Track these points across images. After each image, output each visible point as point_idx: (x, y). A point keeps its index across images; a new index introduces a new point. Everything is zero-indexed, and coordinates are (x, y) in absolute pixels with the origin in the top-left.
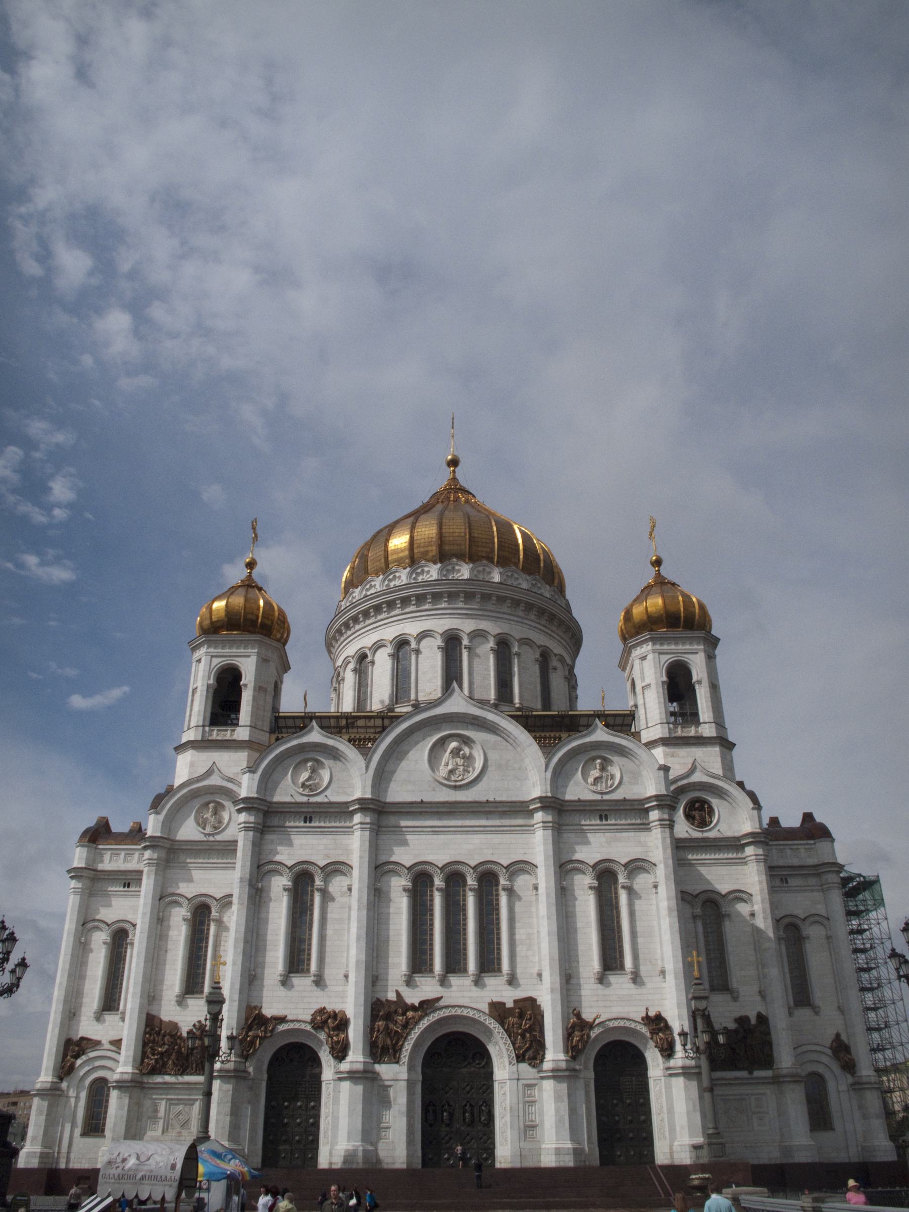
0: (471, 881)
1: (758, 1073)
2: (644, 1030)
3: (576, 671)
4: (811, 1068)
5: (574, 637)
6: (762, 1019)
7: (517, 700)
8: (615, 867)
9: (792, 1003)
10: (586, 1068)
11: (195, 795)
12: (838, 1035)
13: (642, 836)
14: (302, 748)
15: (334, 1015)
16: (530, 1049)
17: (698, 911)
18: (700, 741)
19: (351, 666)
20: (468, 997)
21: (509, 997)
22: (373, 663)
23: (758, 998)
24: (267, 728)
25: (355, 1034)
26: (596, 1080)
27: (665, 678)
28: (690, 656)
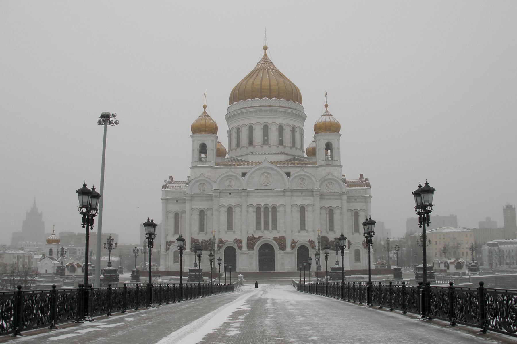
0: (270, 209)
2: (308, 243)
5: (303, 118)
7: (284, 144)
11: (197, 181)
13: (312, 198)
14: (228, 176)
15: (239, 240)
16: (283, 247)
17: (328, 212)
18: (332, 165)
19: (235, 130)
20: (269, 236)
21: (278, 236)
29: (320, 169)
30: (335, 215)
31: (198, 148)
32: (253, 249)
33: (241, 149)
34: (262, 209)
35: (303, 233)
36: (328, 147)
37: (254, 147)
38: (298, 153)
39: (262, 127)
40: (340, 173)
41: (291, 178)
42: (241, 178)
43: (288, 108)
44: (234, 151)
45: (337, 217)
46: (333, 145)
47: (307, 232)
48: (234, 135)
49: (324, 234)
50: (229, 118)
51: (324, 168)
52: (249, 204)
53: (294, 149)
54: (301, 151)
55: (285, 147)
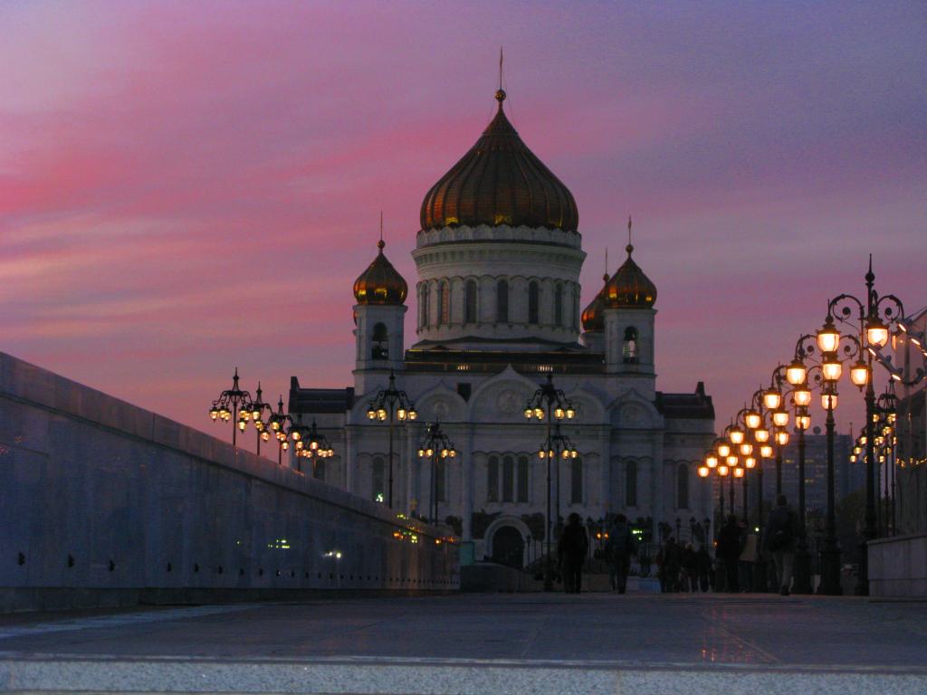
3: (581, 282)
5: (578, 259)
18: (638, 374)
19: (435, 287)
20: (513, 512)
21: (531, 511)
25: (466, 526)
32: (482, 538)
34: (501, 462)
36: (630, 333)
42: (460, 399)
44: (434, 330)
45: (643, 478)
47: (585, 505)
48: (434, 297)
50: (419, 260)
51: (619, 379)
52: (475, 449)
53: (559, 330)
54: (574, 333)
55: (541, 328)
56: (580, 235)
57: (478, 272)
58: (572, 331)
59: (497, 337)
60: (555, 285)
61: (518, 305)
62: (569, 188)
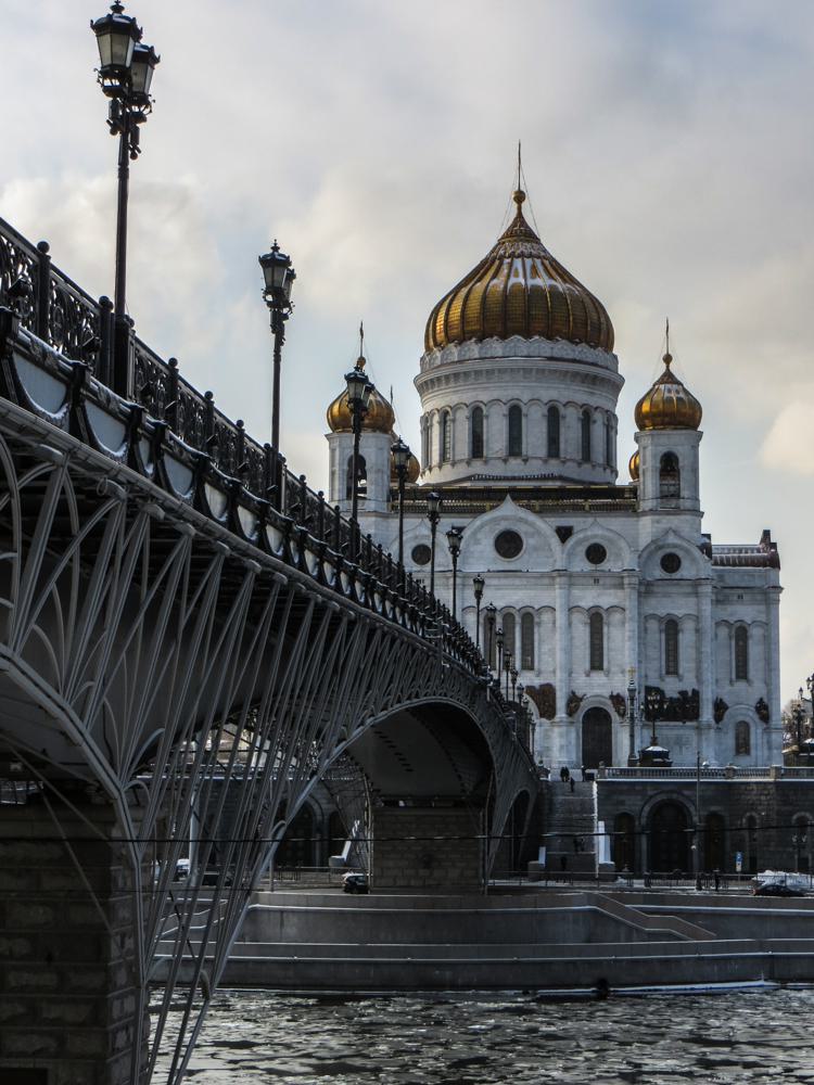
0: (518, 619)
1: (688, 723)
2: (609, 702)
4: (741, 718)
5: (615, 385)
6: (696, 693)
7: (562, 455)
8: (602, 611)
9: (734, 676)
10: (578, 721)
12: (761, 699)
13: (620, 593)
16: (548, 711)
17: (663, 627)
18: (678, 511)
19: (436, 418)
21: (537, 682)
22: (454, 421)
23: (695, 680)
24: (385, 499)
26: (583, 728)
27: (658, 465)
28: (680, 448)
29: (646, 521)
30: (681, 636)
31: (346, 467)
33: (453, 465)
35: (598, 678)
36: (669, 466)
37: (486, 462)
38: (597, 476)
39: (505, 410)
40: (699, 529)
41: (571, 541)
43: (574, 361)
44: (436, 470)
45: (686, 639)
46: (680, 459)
47: (608, 674)
49: (653, 682)
50: (424, 386)
51: (657, 517)
53: (587, 466)
54: (608, 471)
55: (564, 462)
56: (615, 357)
57: (484, 396)
58: (605, 469)
59: (509, 474)
60: (581, 411)
61: (535, 435)
62: (601, 301)
